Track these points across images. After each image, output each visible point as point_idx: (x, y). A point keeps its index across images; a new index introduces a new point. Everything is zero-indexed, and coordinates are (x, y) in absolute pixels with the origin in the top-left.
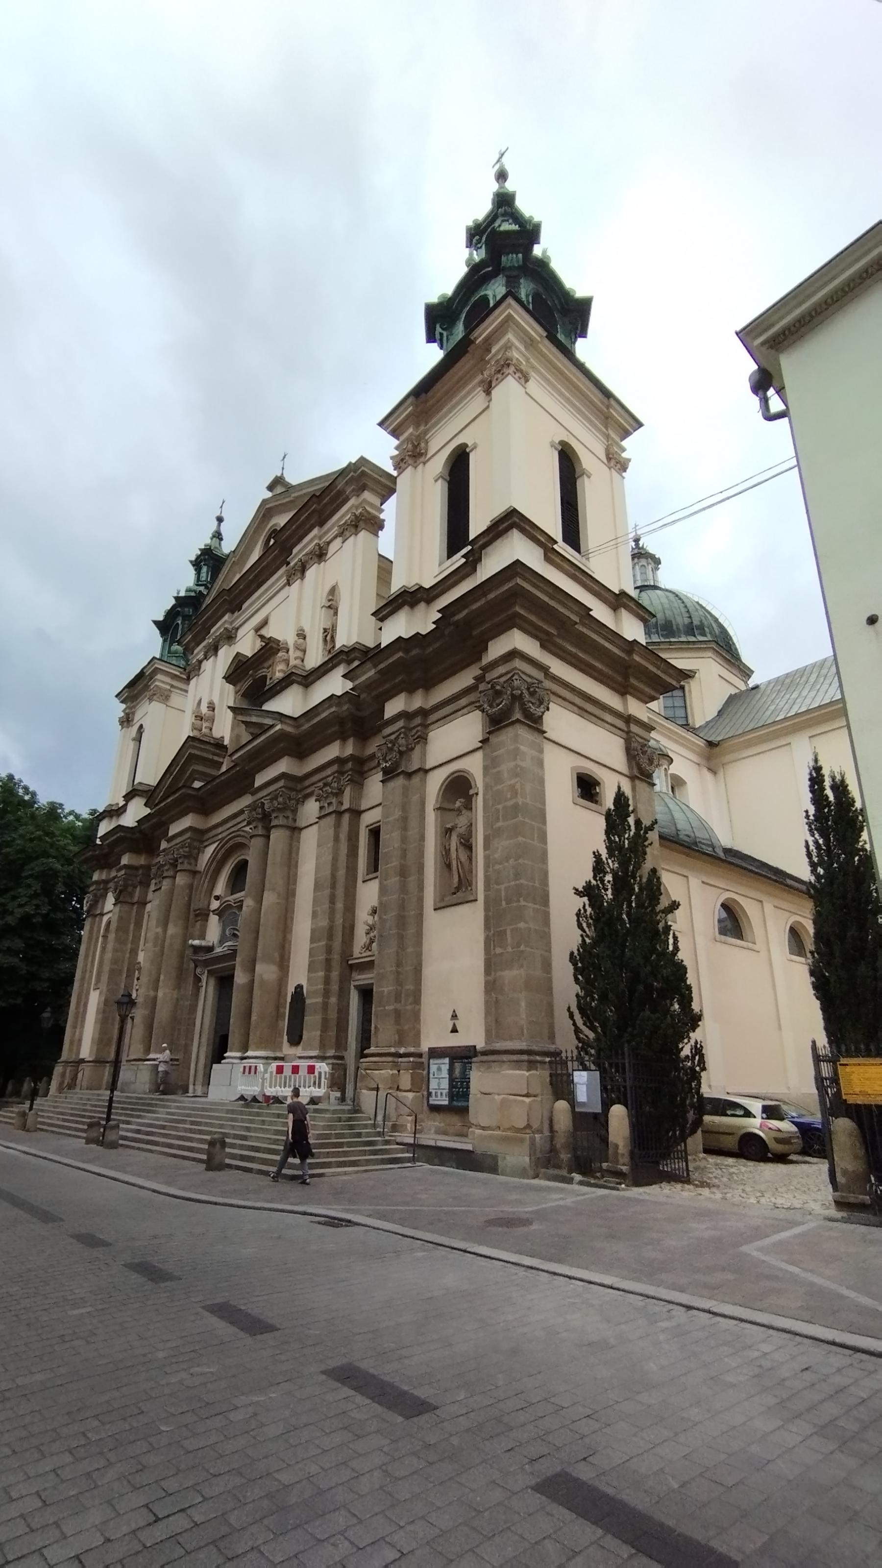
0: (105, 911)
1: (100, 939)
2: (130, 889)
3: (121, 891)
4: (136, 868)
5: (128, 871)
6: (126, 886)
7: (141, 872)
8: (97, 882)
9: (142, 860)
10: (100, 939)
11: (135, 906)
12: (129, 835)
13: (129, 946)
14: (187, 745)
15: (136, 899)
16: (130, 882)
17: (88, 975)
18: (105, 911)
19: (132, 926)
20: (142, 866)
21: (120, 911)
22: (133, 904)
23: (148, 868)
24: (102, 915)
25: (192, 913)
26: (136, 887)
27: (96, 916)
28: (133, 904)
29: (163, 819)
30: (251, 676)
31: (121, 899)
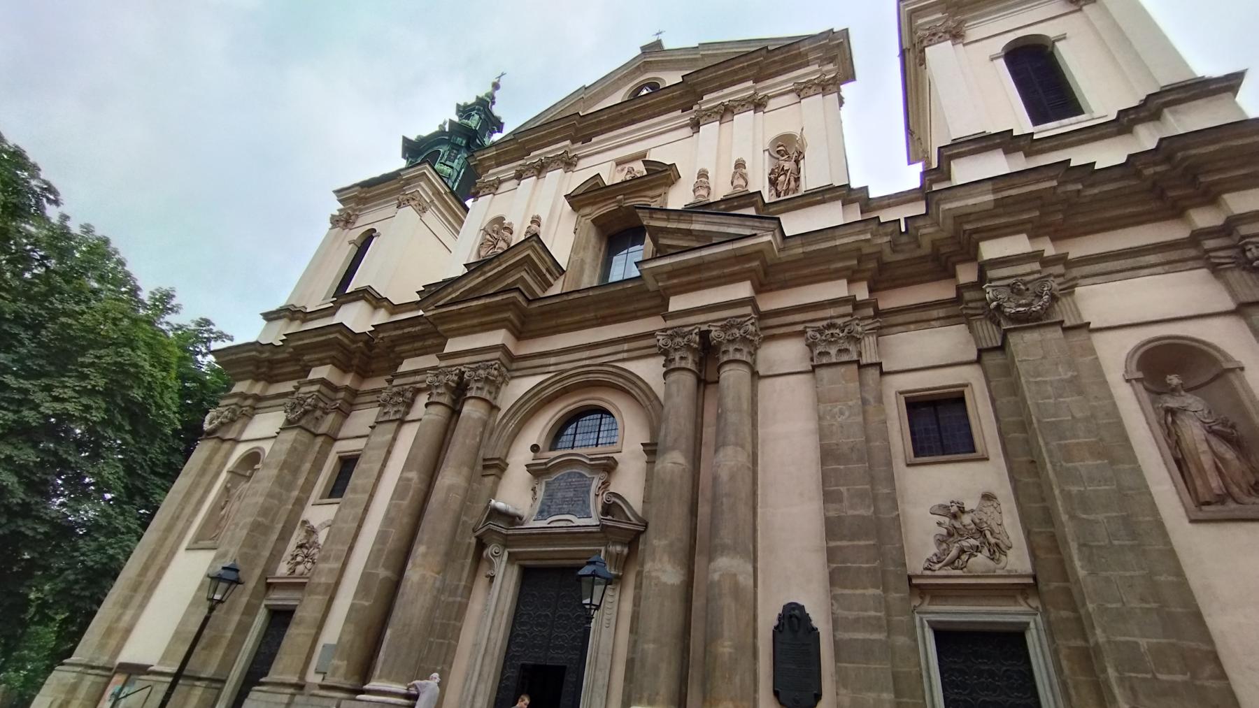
0: (244, 437)
1: (224, 476)
2: (318, 413)
3: (306, 413)
4: (336, 389)
5: (324, 389)
6: (315, 407)
7: (342, 395)
8: (244, 396)
9: (348, 380)
10: (224, 476)
11: (320, 440)
12: (346, 341)
13: (295, 493)
14: (527, 244)
15: (320, 431)
16: (321, 405)
17: (180, 525)
18: (244, 437)
19: (307, 466)
20: (347, 388)
21: (295, 441)
22: (316, 435)
23: (354, 393)
24: (236, 441)
25: (480, 462)
26: (327, 414)
27: (223, 441)
28: (316, 435)
29: (440, 328)
30: (620, 201)
31: (303, 422)
